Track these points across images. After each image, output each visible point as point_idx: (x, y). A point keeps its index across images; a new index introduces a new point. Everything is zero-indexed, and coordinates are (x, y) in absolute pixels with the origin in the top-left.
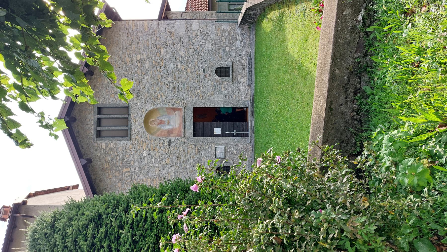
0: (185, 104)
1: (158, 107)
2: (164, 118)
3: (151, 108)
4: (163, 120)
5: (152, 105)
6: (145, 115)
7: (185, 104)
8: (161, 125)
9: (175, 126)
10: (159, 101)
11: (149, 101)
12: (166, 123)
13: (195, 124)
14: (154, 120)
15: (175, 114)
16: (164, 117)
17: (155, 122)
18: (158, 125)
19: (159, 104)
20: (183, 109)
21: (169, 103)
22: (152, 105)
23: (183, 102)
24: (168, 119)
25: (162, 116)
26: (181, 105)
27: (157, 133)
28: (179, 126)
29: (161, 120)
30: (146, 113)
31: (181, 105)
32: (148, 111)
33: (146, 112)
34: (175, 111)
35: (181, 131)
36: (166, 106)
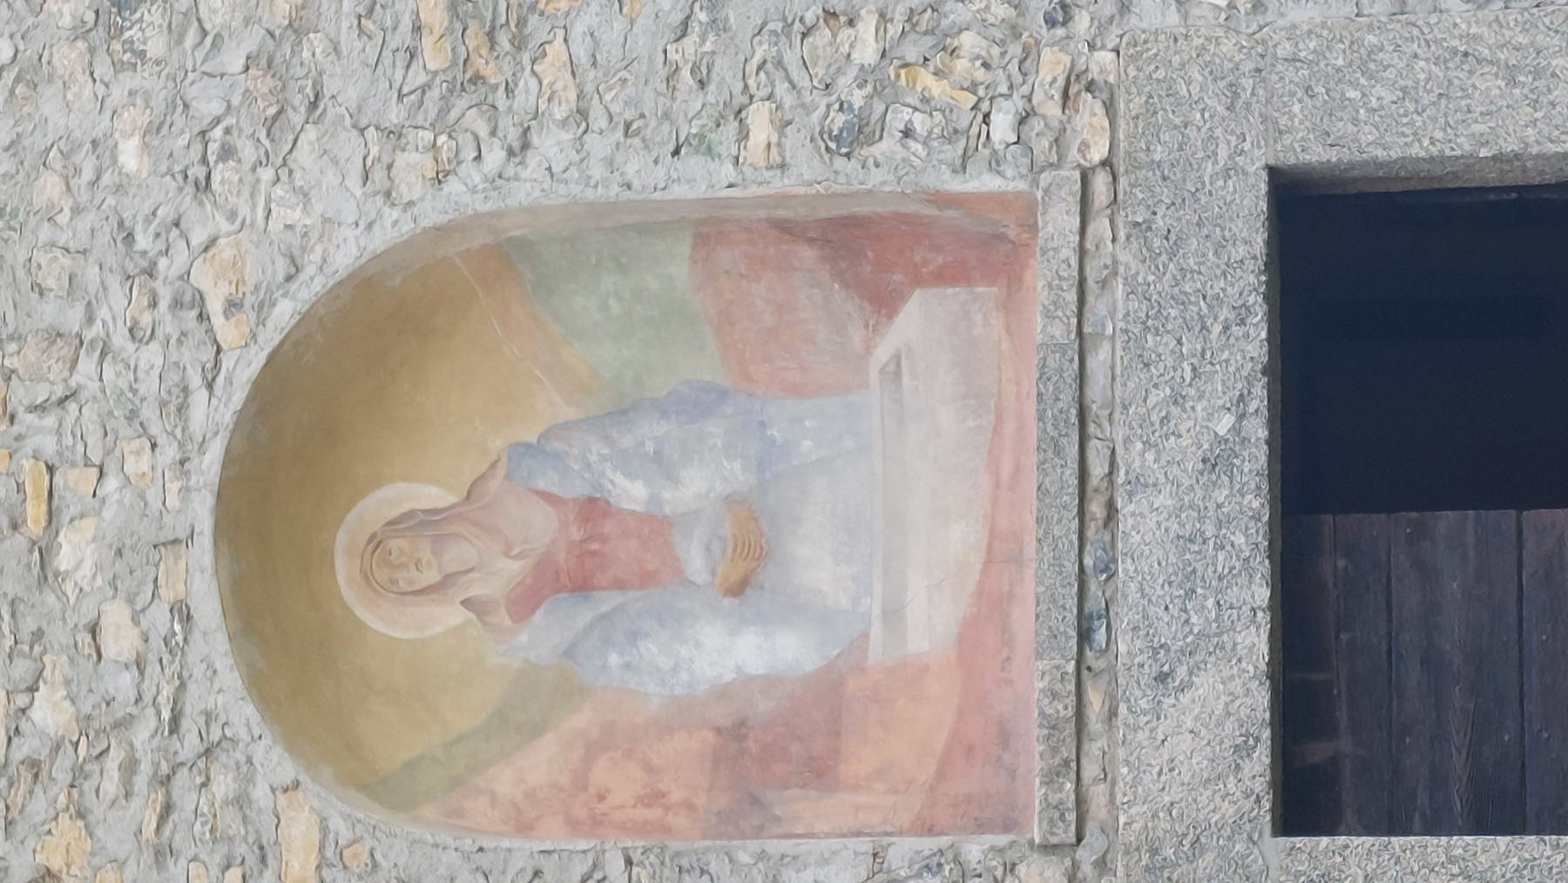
0: (1090, 112)
1: (529, 186)
2: (662, 466)
3: (392, 229)
4: (630, 493)
5: (413, 165)
6: (243, 369)
7: (1090, 112)
8: (585, 614)
9: (894, 615)
10: (552, 68)
11: (346, 88)
12: (696, 563)
13: (1333, 566)
14: (430, 496)
15: (894, 373)
16: (650, 432)
17: (458, 555)
18: (526, 601)
19: (551, 144)
20: (1060, 220)
21: (759, 119)
22: (413, 165)
23: (1052, 65)
24: (737, 474)
25: (622, 412)
26: (1002, 127)
27: (504, 781)
28: (968, 640)
29: (594, 509)
30: (270, 337)
31: (1002, 127)
32: (312, 287)
33: (285, 312)
34: (884, 303)
35: (1005, 735)
36: (692, 163)
